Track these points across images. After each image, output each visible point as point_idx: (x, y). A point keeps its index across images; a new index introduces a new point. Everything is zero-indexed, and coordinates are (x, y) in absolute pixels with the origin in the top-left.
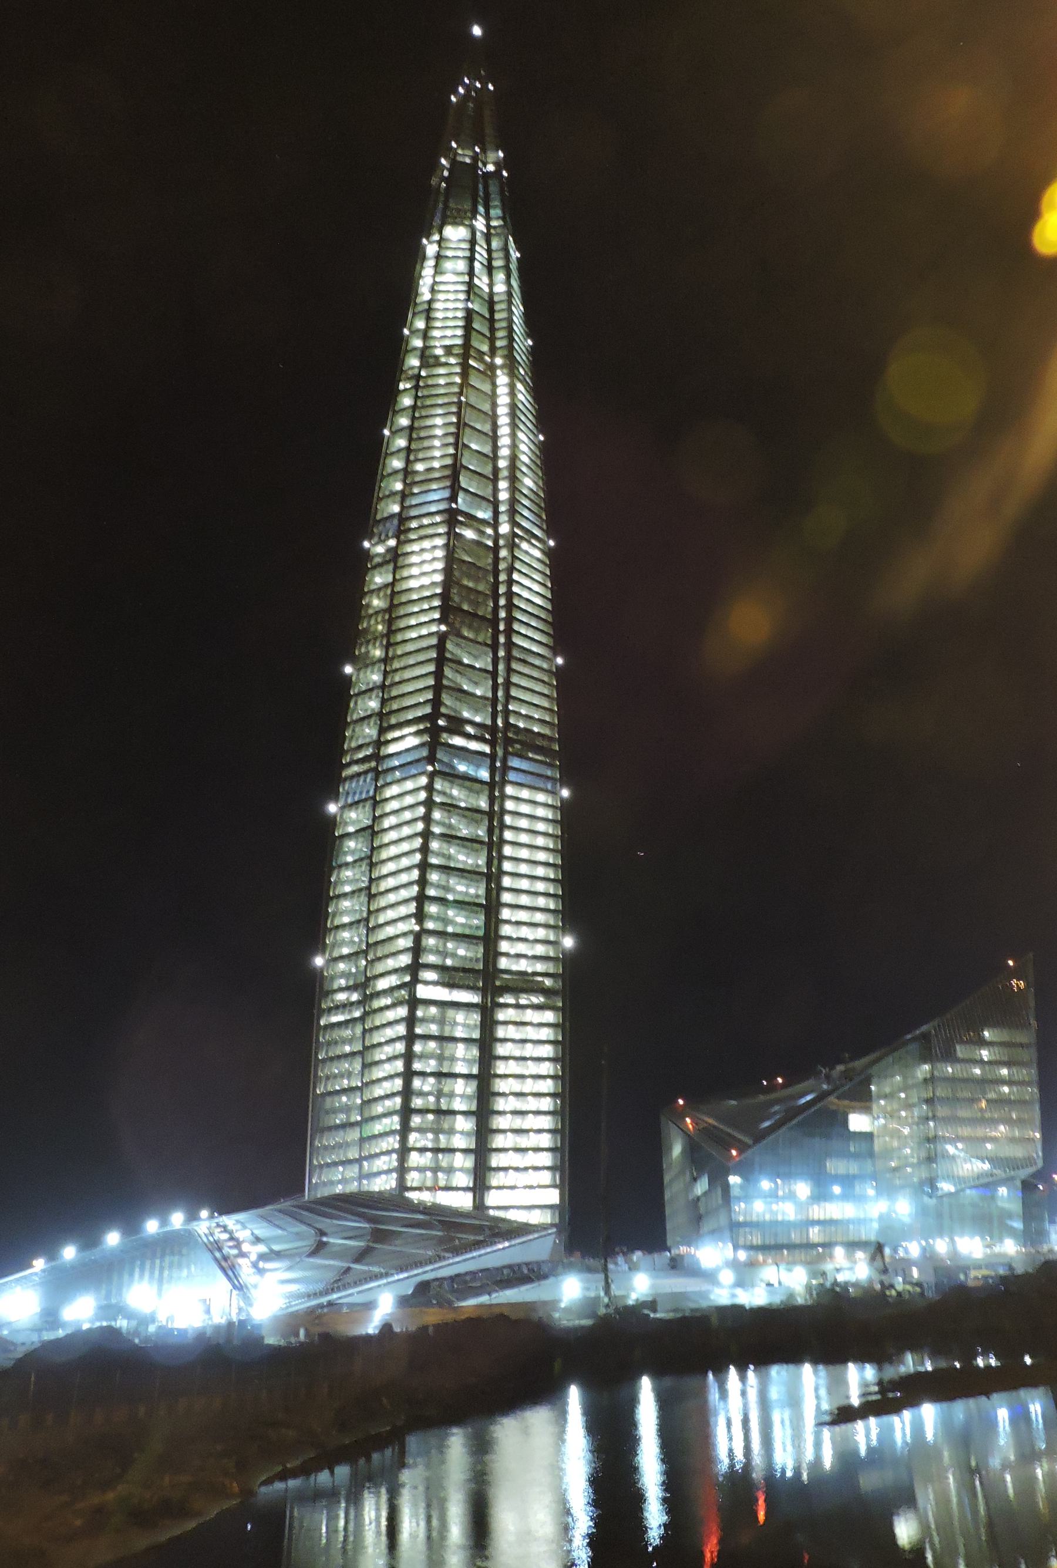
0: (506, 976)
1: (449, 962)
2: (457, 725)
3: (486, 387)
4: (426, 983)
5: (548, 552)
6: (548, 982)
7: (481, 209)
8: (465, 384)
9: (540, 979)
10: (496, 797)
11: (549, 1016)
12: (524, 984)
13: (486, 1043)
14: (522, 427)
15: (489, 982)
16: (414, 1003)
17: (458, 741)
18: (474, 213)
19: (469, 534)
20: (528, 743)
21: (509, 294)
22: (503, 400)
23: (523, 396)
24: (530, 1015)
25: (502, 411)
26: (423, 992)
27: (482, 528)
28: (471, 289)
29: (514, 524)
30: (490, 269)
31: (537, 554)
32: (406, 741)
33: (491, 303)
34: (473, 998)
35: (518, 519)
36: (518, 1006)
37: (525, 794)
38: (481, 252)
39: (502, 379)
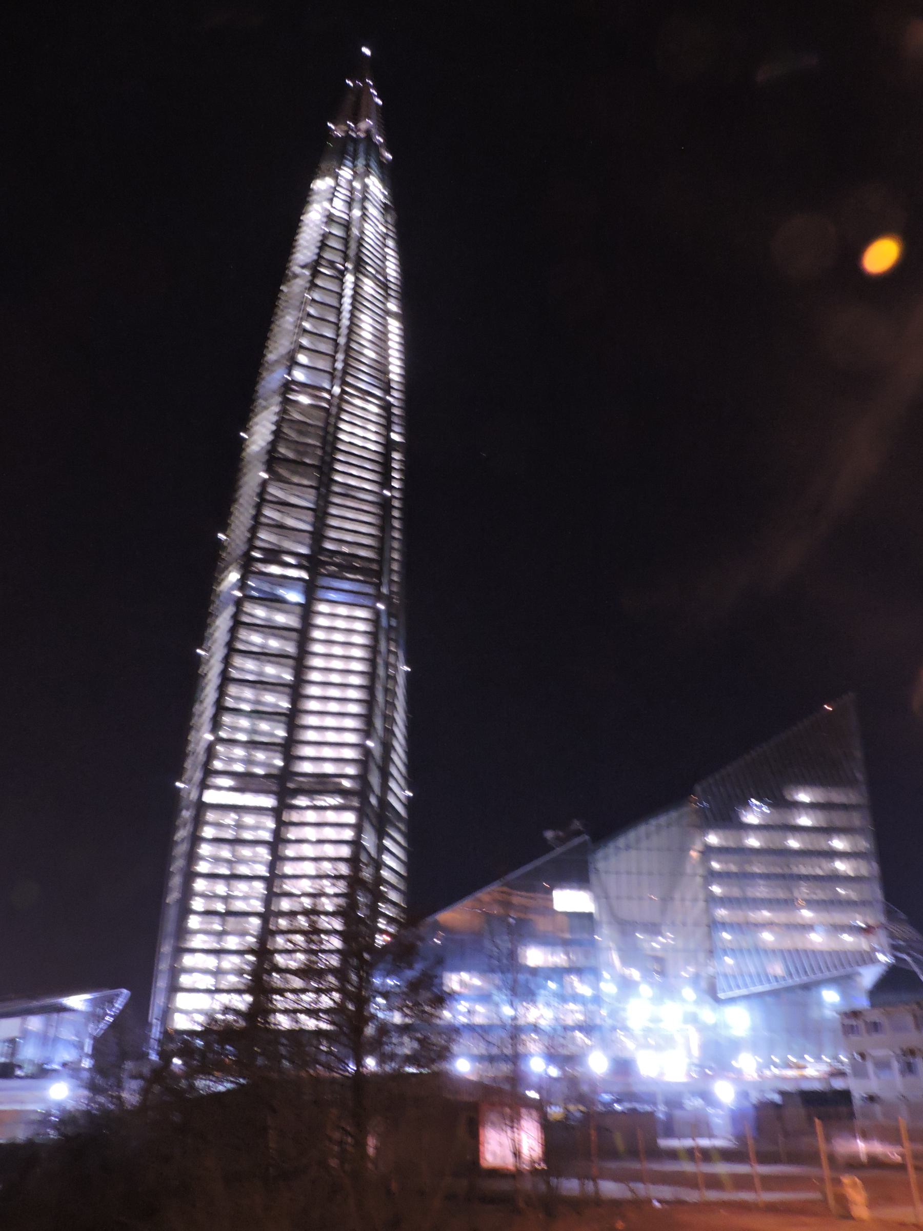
0: (301, 779)
1: (260, 771)
2: (273, 555)
3: (333, 286)
4: (219, 788)
5: (387, 407)
6: (347, 784)
8: (313, 286)
9: (337, 780)
10: (307, 612)
11: (350, 817)
12: (322, 785)
13: (277, 843)
14: (366, 311)
15: (285, 786)
16: (201, 807)
17: (274, 569)
18: (340, 164)
19: (304, 400)
20: (347, 564)
21: (364, 216)
22: (348, 292)
23: (369, 287)
24: (331, 816)
25: (347, 302)
26: (210, 797)
27: (318, 393)
28: (330, 219)
29: (344, 383)
30: (350, 204)
31: (375, 410)
32: (233, 576)
33: (347, 226)
34: (268, 802)
35: (350, 380)
36: (315, 808)
37: (342, 610)
38: (343, 193)
39: (349, 279)
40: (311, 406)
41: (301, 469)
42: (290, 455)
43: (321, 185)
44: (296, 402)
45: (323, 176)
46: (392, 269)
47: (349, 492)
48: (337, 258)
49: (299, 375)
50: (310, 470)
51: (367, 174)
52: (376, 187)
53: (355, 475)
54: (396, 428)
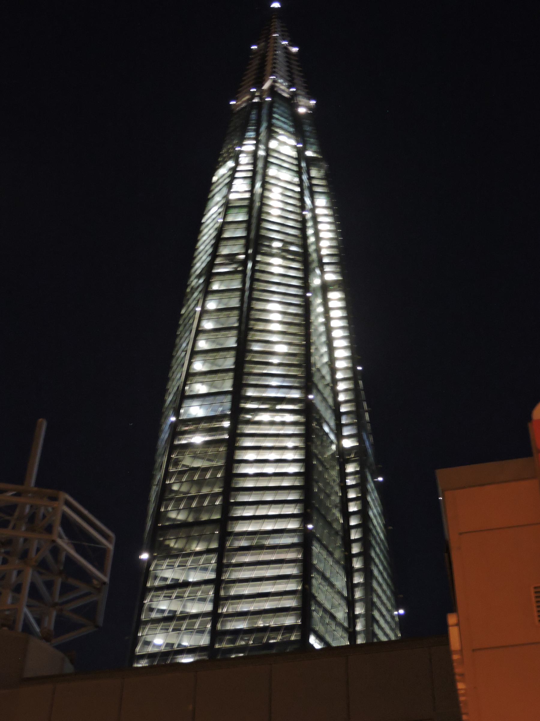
7: (252, 134)
14: (276, 298)
27: (217, 425)
40: (207, 444)
41: (195, 532)
42: (181, 517)
43: (223, 171)
45: (225, 162)
46: (325, 236)
47: (258, 542)
48: (236, 248)
49: (195, 410)
50: (208, 530)
51: (271, 134)
52: (285, 145)
53: (269, 516)
54: (346, 432)
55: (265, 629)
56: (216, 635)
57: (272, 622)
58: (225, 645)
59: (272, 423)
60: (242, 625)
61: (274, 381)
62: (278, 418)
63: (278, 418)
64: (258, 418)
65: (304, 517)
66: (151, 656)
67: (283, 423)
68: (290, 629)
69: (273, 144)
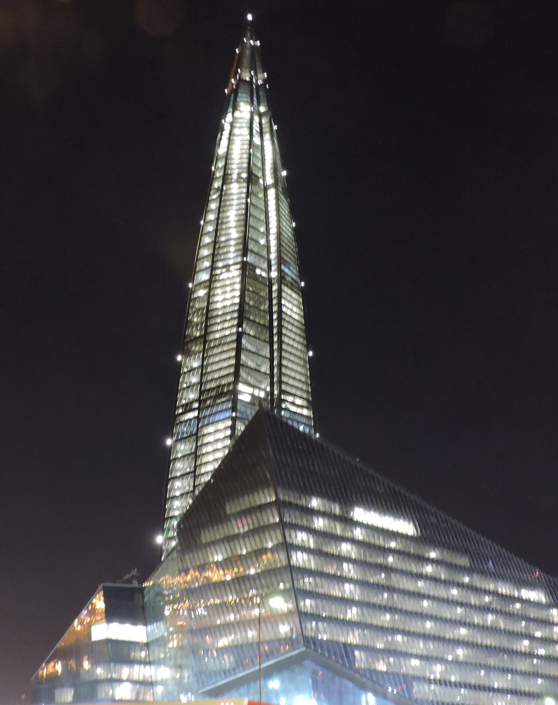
37: (221, 426)
44: (198, 297)
54: (274, 268)
55: (219, 387)
56: (201, 393)
57: (224, 382)
58: (205, 396)
59: (228, 278)
60: (213, 385)
61: (232, 255)
62: (230, 275)
63: (230, 275)
64: (221, 277)
65: (239, 325)
66: (183, 406)
67: (234, 277)
68: (229, 384)
69: (237, 114)
